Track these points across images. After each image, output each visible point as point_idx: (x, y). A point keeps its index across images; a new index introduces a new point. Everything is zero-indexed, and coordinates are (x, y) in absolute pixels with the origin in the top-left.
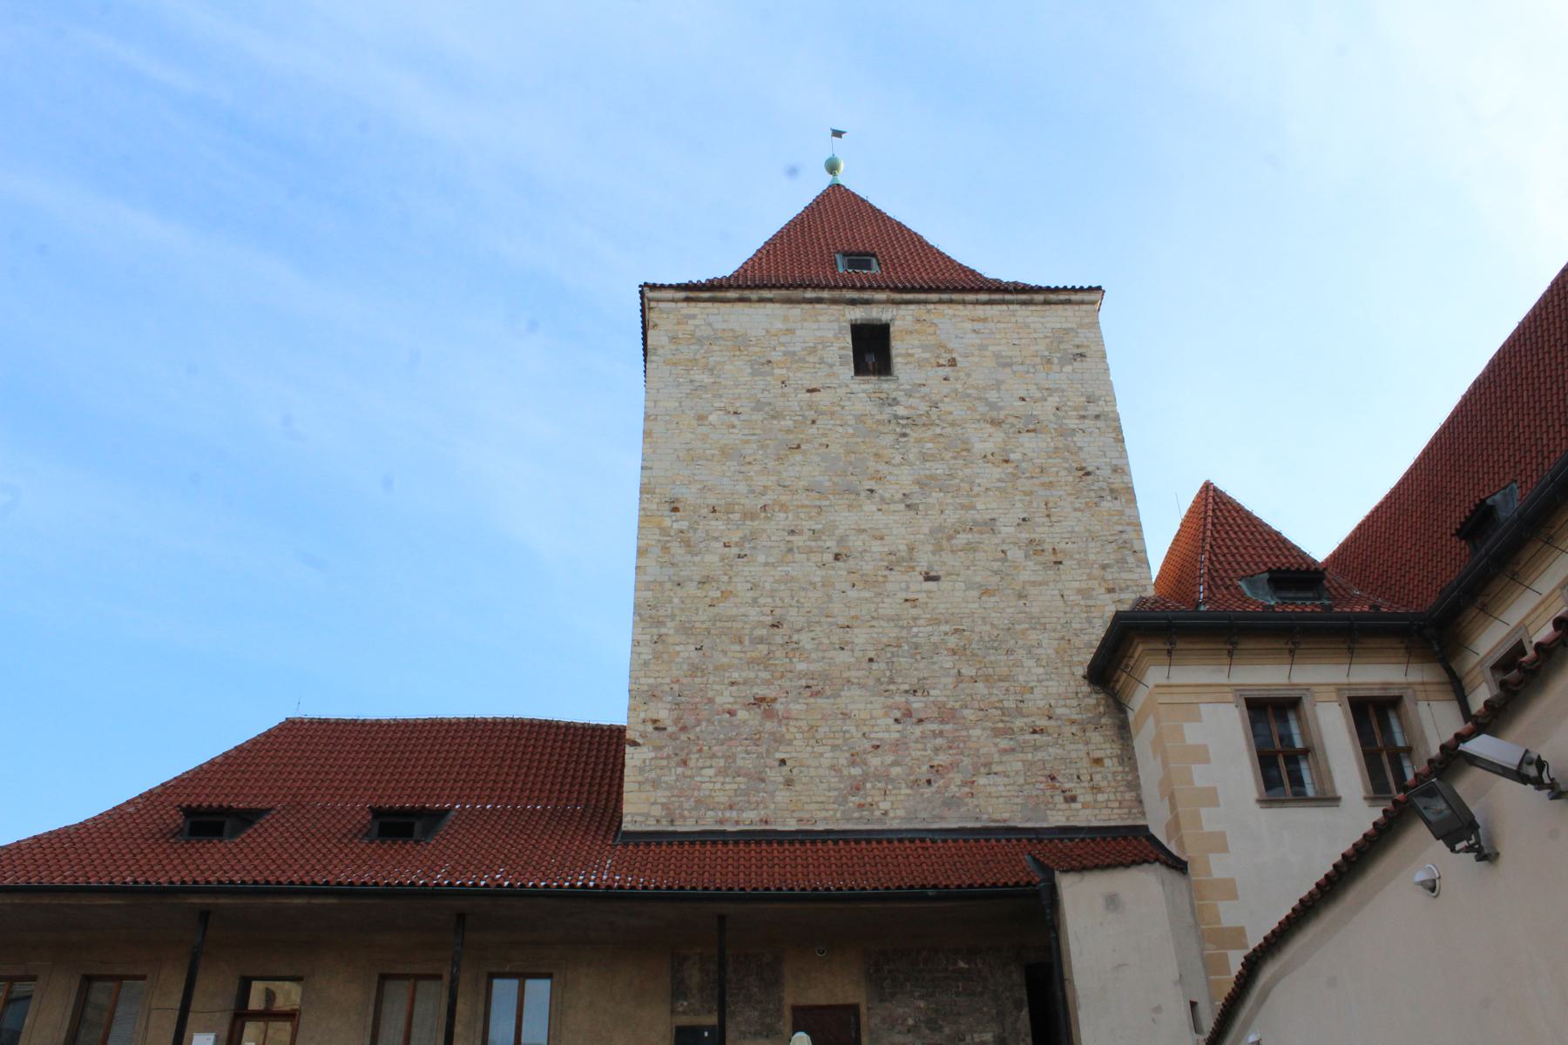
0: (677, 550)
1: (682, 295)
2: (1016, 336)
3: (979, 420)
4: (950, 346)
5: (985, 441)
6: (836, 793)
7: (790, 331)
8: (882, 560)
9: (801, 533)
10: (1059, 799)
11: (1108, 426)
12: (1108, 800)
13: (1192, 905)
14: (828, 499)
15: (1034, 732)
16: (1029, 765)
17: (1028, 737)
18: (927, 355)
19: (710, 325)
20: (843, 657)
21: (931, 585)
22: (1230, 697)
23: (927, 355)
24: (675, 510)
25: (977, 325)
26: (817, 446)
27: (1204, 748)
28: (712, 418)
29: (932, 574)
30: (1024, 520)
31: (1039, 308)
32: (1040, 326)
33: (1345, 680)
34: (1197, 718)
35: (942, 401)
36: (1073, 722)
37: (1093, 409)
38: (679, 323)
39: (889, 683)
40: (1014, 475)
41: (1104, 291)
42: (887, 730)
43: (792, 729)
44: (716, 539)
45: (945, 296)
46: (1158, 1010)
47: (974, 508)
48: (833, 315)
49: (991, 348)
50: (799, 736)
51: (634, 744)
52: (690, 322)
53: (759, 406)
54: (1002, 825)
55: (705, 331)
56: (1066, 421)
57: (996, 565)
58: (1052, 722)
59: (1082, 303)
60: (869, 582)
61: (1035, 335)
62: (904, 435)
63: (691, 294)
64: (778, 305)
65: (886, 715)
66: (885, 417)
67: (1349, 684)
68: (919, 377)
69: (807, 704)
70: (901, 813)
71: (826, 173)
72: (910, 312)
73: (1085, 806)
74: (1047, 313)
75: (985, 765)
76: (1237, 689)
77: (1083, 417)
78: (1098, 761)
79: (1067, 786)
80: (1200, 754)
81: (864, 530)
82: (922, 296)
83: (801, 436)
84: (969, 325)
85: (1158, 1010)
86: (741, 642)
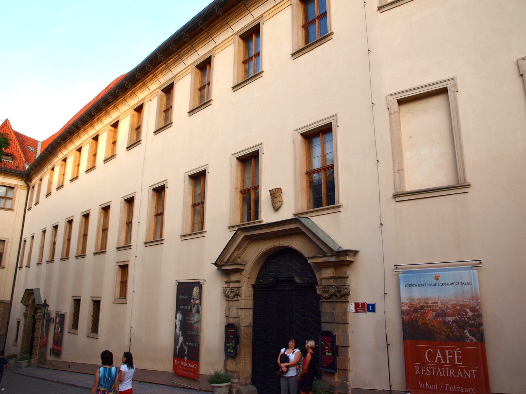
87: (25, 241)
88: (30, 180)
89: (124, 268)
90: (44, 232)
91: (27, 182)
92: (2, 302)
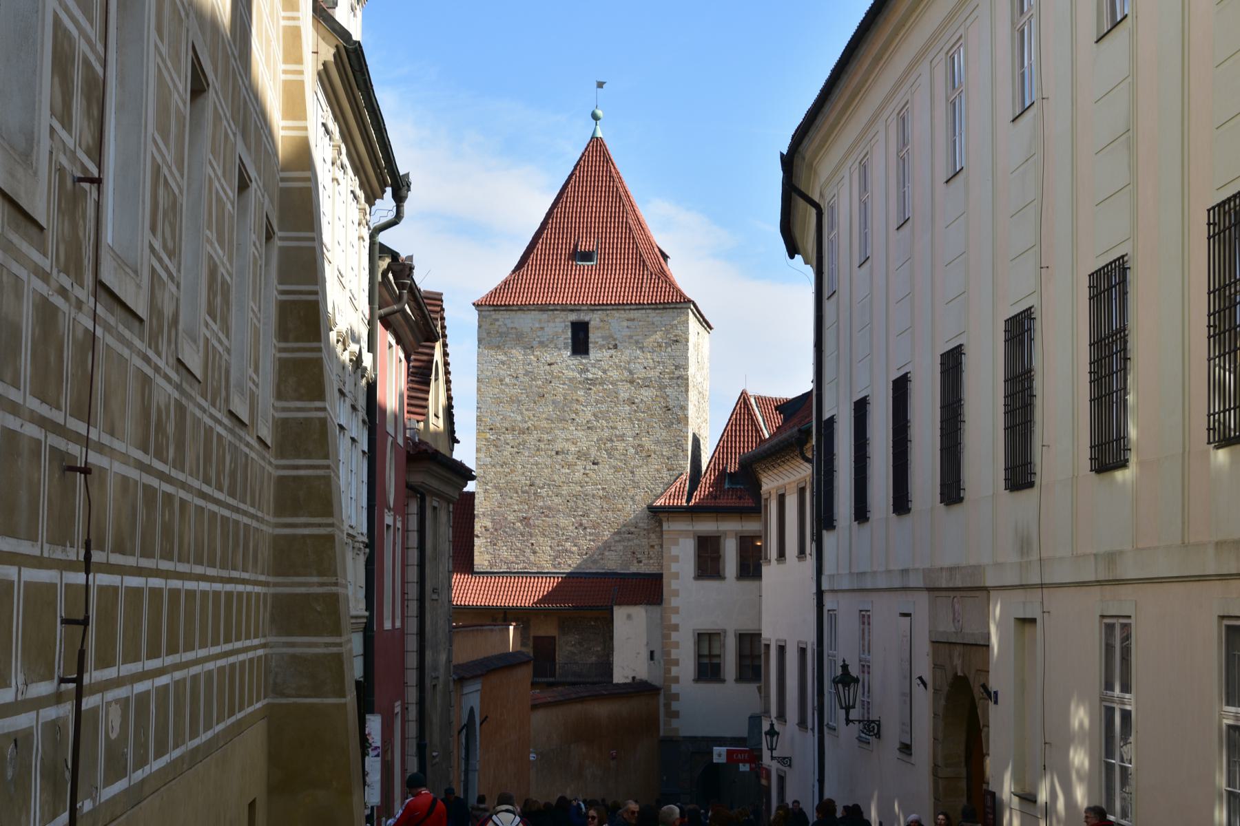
0: (493, 449)
2: (646, 329)
3: (624, 380)
4: (615, 337)
5: (625, 392)
6: (552, 557)
7: (542, 328)
8: (575, 454)
9: (543, 441)
10: (635, 561)
11: (682, 383)
13: (661, 616)
15: (629, 533)
16: (625, 547)
17: (626, 536)
18: (604, 342)
19: (505, 325)
20: (557, 500)
21: (596, 467)
22: (692, 536)
23: (604, 342)
24: (491, 429)
25: (630, 323)
26: (551, 395)
27: (678, 556)
28: (507, 380)
29: (596, 461)
30: (637, 434)
31: (661, 311)
32: (659, 323)
34: (677, 544)
36: (645, 530)
37: (677, 373)
40: (635, 411)
41: (693, 302)
43: (537, 531)
44: (508, 444)
45: (615, 307)
46: (638, 653)
47: (616, 428)
48: (562, 318)
49: (634, 338)
51: (478, 537)
52: (497, 323)
53: (527, 373)
54: (612, 571)
55: (504, 329)
56: (663, 381)
60: (569, 466)
61: (656, 329)
62: (590, 389)
63: (496, 308)
64: (537, 312)
65: (573, 525)
67: (742, 531)
68: (599, 356)
69: (543, 520)
70: (575, 565)
73: (644, 565)
74: (664, 315)
76: (695, 533)
77: (673, 378)
78: (652, 546)
79: (639, 556)
80: (676, 559)
83: (545, 390)
84: (625, 324)
85: (638, 653)
86: (517, 493)
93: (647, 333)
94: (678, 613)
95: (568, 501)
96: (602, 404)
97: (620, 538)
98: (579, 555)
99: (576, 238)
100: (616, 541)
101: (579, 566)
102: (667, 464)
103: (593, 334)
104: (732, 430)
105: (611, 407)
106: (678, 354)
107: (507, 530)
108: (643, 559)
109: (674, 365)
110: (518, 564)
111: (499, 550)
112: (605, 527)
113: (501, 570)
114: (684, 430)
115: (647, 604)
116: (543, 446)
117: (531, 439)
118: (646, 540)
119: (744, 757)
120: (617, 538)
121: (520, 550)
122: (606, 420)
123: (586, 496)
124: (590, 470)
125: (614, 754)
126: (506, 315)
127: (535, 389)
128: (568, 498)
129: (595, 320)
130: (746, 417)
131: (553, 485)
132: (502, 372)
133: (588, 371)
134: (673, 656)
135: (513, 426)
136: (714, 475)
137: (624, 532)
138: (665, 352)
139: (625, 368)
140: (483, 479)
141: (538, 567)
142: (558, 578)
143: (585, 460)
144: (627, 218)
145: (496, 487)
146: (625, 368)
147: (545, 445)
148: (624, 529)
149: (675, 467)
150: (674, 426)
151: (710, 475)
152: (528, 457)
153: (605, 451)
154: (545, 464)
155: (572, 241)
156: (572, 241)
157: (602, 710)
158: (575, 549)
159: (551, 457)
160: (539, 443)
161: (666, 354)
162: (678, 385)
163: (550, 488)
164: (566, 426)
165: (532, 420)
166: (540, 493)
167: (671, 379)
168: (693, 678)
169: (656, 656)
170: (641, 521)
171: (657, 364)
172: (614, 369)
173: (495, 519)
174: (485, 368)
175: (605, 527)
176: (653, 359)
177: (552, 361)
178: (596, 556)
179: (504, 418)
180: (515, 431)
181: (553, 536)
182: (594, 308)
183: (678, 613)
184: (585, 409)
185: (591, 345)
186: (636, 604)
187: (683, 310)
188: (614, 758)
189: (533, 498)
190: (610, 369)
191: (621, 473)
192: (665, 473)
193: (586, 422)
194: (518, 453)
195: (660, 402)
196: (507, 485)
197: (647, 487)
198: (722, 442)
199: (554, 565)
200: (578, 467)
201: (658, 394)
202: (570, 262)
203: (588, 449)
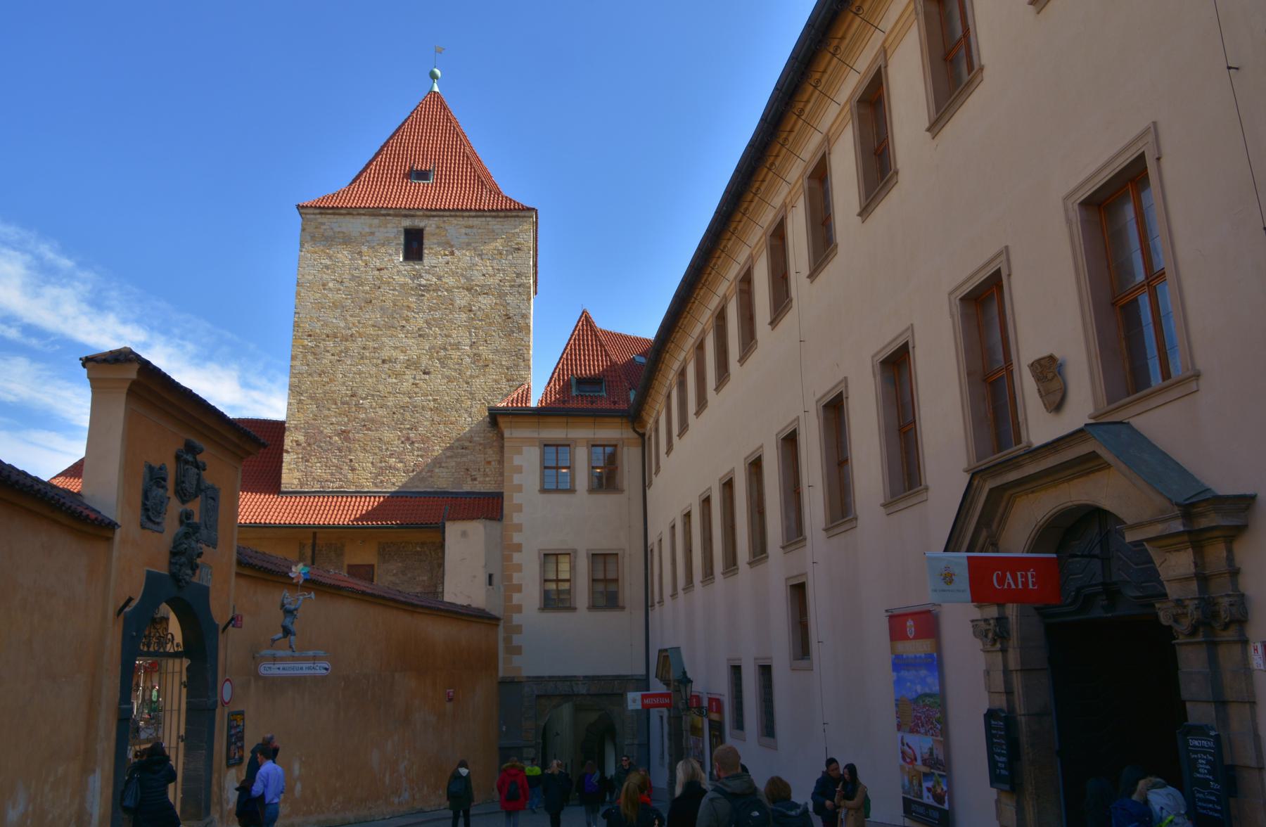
0: (310, 357)
1: (317, 211)
4: (452, 243)
5: (462, 299)
7: (372, 234)
9: (369, 349)
10: (469, 479)
12: (491, 481)
14: (381, 330)
15: (463, 449)
19: (332, 229)
20: (381, 412)
21: (427, 377)
24: (310, 336)
25: (468, 231)
27: (521, 466)
28: (331, 285)
30: (474, 343)
33: (592, 436)
34: (520, 453)
35: (444, 277)
36: (480, 444)
38: (316, 228)
39: (401, 424)
40: (472, 318)
41: (537, 210)
42: (397, 446)
43: (357, 446)
44: (328, 351)
45: (453, 213)
46: (475, 577)
47: (451, 336)
49: (473, 244)
50: (359, 448)
51: (288, 452)
53: (353, 278)
55: (330, 233)
57: (457, 367)
58: (470, 444)
59: (524, 217)
60: (397, 375)
62: (423, 296)
63: (323, 211)
64: (367, 217)
65: (399, 439)
66: (415, 285)
68: (434, 262)
70: (400, 484)
71: (429, 78)
72: (434, 222)
75: (439, 463)
77: (513, 286)
78: (489, 463)
79: (473, 474)
80: (519, 470)
81: (397, 347)
82: (441, 213)
83: (373, 296)
84: (463, 231)
85: (475, 577)
86: (336, 404)
87: (652, 550)
88: (643, 425)
89: (799, 591)
90: (673, 527)
91: (638, 430)
92: (630, 678)
93: (486, 241)
94: (521, 531)
95: (394, 413)
96: (435, 311)
97: (452, 453)
98: (404, 472)
99: (412, 162)
100: (448, 457)
101: (404, 485)
102: (506, 374)
103: (428, 240)
104: (575, 345)
105: (446, 315)
106: (519, 262)
107: (322, 445)
108: (478, 476)
109: (515, 272)
110: (333, 482)
111: (312, 467)
112: (436, 441)
113: (313, 490)
114: (525, 339)
115: (486, 518)
116: (368, 354)
117: (354, 347)
118: (482, 456)
119: (1025, 584)
120: (449, 454)
121: (337, 467)
122: (439, 328)
123: (415, 407)
124: (421, 379)
125: (451, 694)
126: (334, 219)
127: (361, 295)
128: (394, 410)
129: (431, 225)
130: (589, 333)
131: (377, 396)
132: (325, 276)
133: (422, 277)
134: (515, 581)
135: (334, 332)
136: (559, 385)
137: (457, 447)
138: (506, 259)
139: (462, 275)
140: (298, 389)
141: (356, 486)
142: (379, 497)
143: (415, 369)
144: (464, 149)
145: (311, 398)
146: (462, 275)
147: (370, 353)
148: (457, 444)
149: (515, 377)
150: (515, 334)
151: (555, 385)
152: (351, 365)
153: (438, 359)
154: (370, 374)
155: (408, 164)
156: (408, 164)
157: (438, 631)
158: (400, 465)
159: (377, 365)
160: (363, 351)
161: (507, 262)
162: (519, 293)
163: (374, 399)
164: (395, 333)
165: (357, 327)
166: (362, 404)
167: (512, 286)
168: (538, 606)
169: (496, 580)
170: (477, 435)
171: (496, 271)
172: (450, 276)
173: (308, 433)
174: (307, 272)
175: (436, 441)
176: (492, 267)
177: (382, 266)
178: (424, 473)
179: (326, 324)
180: (337, 338)
181: (375, 451)
182: (431, 213)
183: (521, 531)
184: (417, 316)
185: (426, 251)
186: (472, 518)
187: (525, 219)
188: (450, 700)
189: (354, 409)
190: (446, 275)
191: (455, 384)
192: (504, 384)
193: (417, 329)
194: (339, 361)
195: (499, 311)
196: (325, 396)
197: (484, 398)
198: (565, 355)
199: (375, 483)
200: (406, 377)
201: (498, 301)
202: (405, 180)
203: (419, 358)
